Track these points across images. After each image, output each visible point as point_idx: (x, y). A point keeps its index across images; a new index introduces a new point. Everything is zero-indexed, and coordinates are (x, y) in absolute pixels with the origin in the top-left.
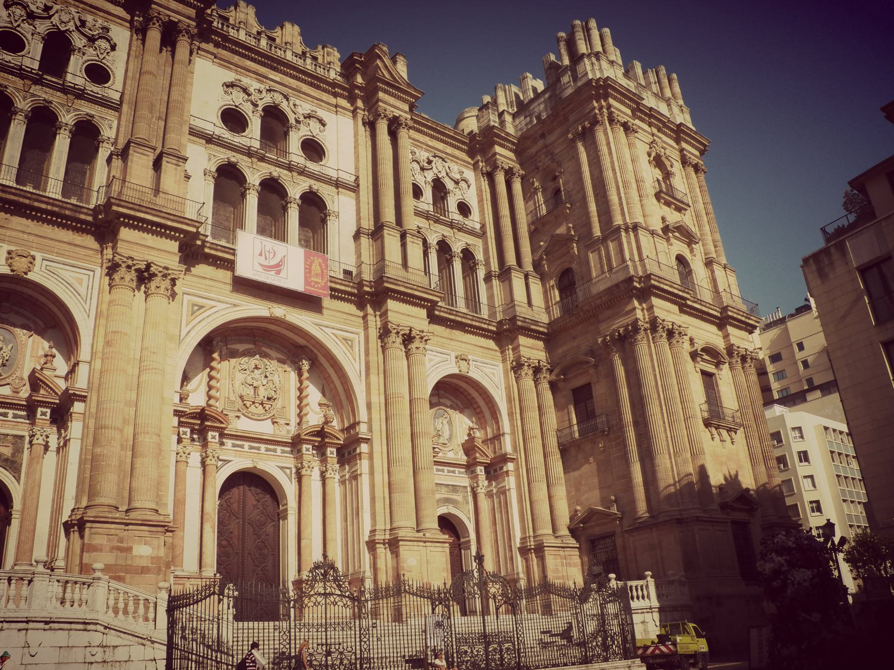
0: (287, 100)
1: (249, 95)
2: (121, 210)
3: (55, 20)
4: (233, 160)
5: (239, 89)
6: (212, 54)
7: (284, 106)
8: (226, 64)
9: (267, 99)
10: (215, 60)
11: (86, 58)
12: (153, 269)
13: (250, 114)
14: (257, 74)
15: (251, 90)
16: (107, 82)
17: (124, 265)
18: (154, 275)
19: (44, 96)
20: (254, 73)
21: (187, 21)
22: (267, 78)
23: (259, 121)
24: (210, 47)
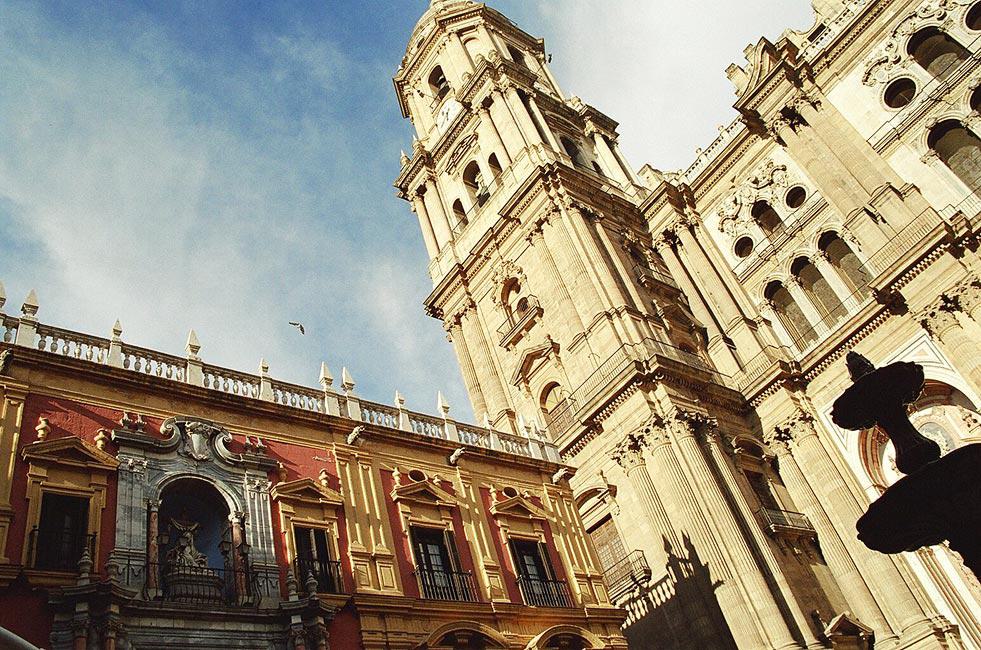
0: (915, 15)
1: (887, 61)
2: (884, 284)
3: (745, 201)
4: (931, 123)
5: (875, 69)
6: (833, 76)
7: (920, 24)
8: (848, 66)
9: (902, 42)
10: (840, 76)
11: (780, 198)
12: (950, 296)
13: (904, 71)
14: (875, 37)
15: (885, 54)
16: (805, 193)
17: (928, 317)
18: (956, 298)
19: (789, 254)
20: (871, 40)
21: (789, 94)
22: (883, 28)
23: (916, 65)
24: (828, 73)
